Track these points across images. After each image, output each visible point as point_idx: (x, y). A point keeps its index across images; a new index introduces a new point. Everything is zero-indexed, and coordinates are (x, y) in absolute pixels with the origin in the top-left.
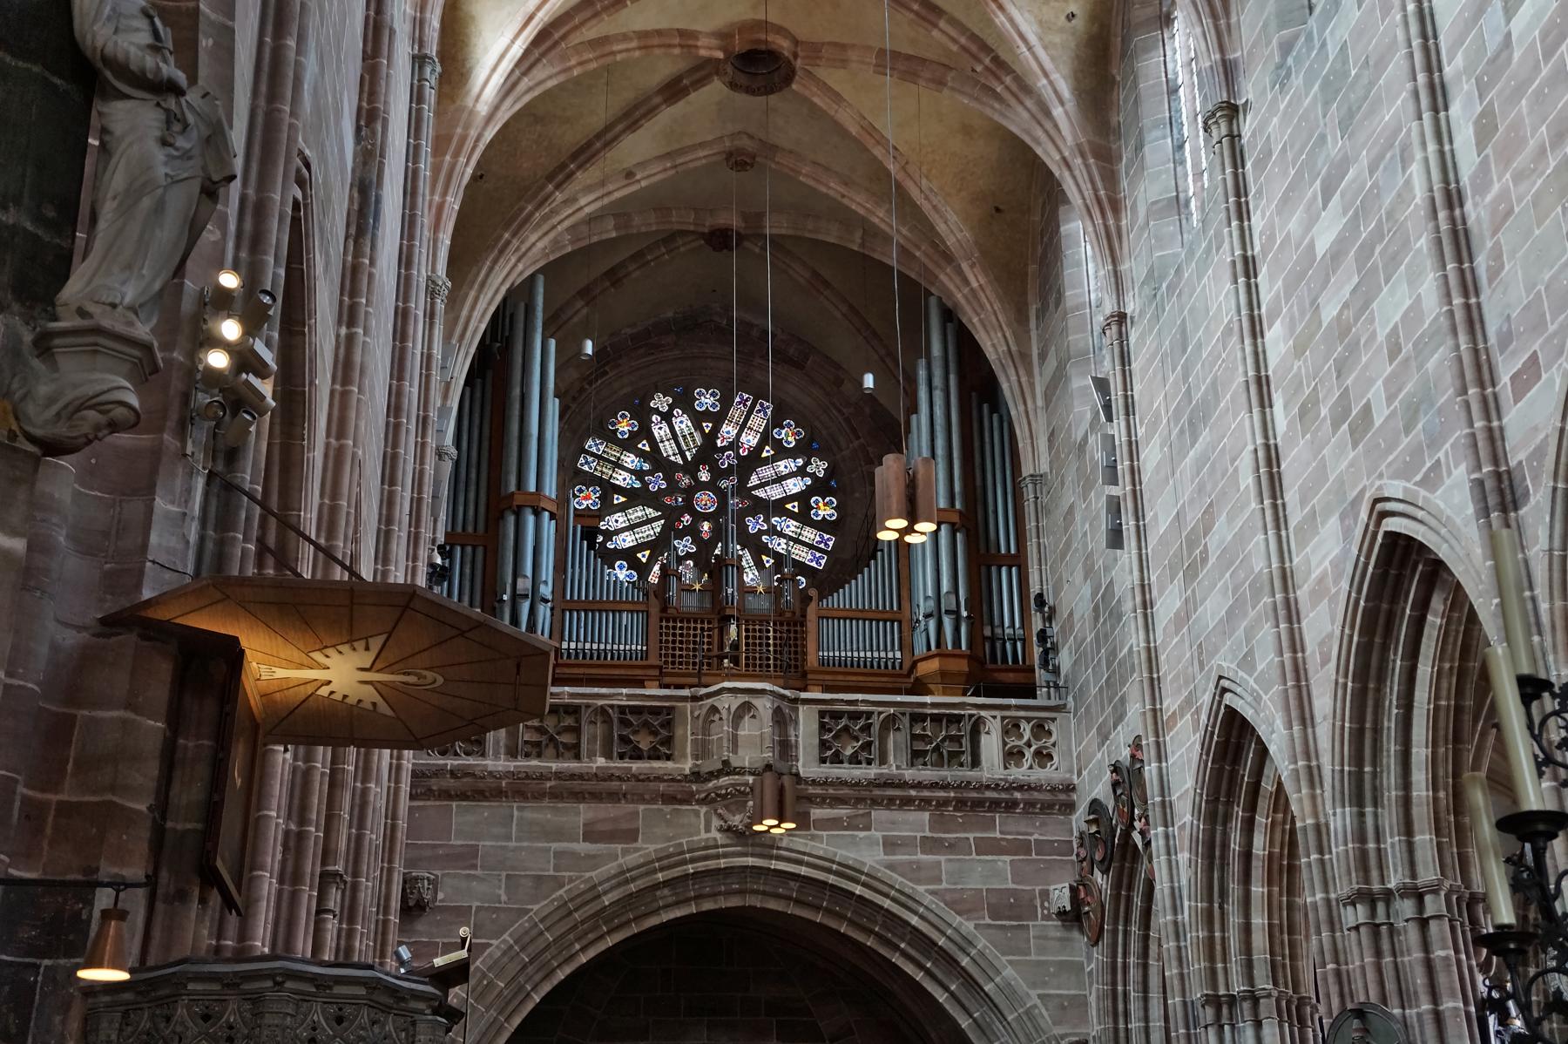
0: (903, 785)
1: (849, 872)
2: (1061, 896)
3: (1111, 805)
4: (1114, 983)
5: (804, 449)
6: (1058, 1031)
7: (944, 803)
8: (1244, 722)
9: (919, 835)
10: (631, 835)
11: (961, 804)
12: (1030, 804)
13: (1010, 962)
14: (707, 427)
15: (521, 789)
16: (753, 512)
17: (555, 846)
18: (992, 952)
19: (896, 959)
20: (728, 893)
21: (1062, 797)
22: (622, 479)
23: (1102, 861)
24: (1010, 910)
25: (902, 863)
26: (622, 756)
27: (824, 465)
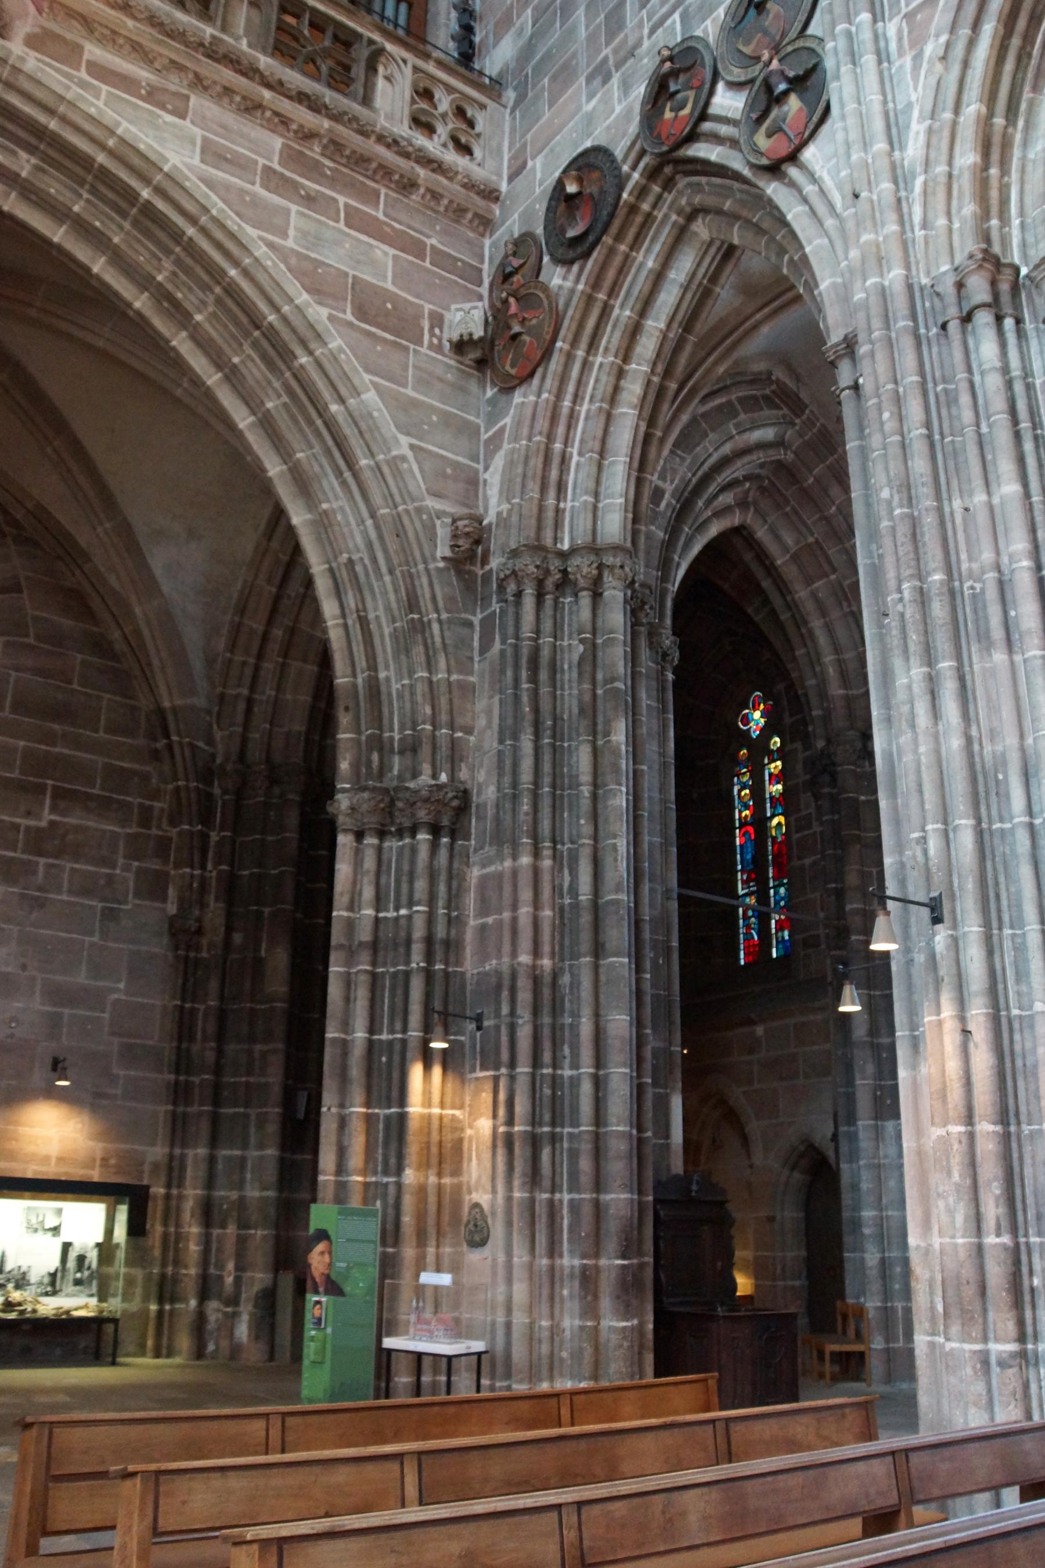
0: (250, 72)
4: (550, 437)
6: (431, 503)
7: (308, 136)
9: (262, 161)
11: (335, 147)
13: (376, 385)
18: (349, 360)
19: (181, 343)
25: (228, 187)
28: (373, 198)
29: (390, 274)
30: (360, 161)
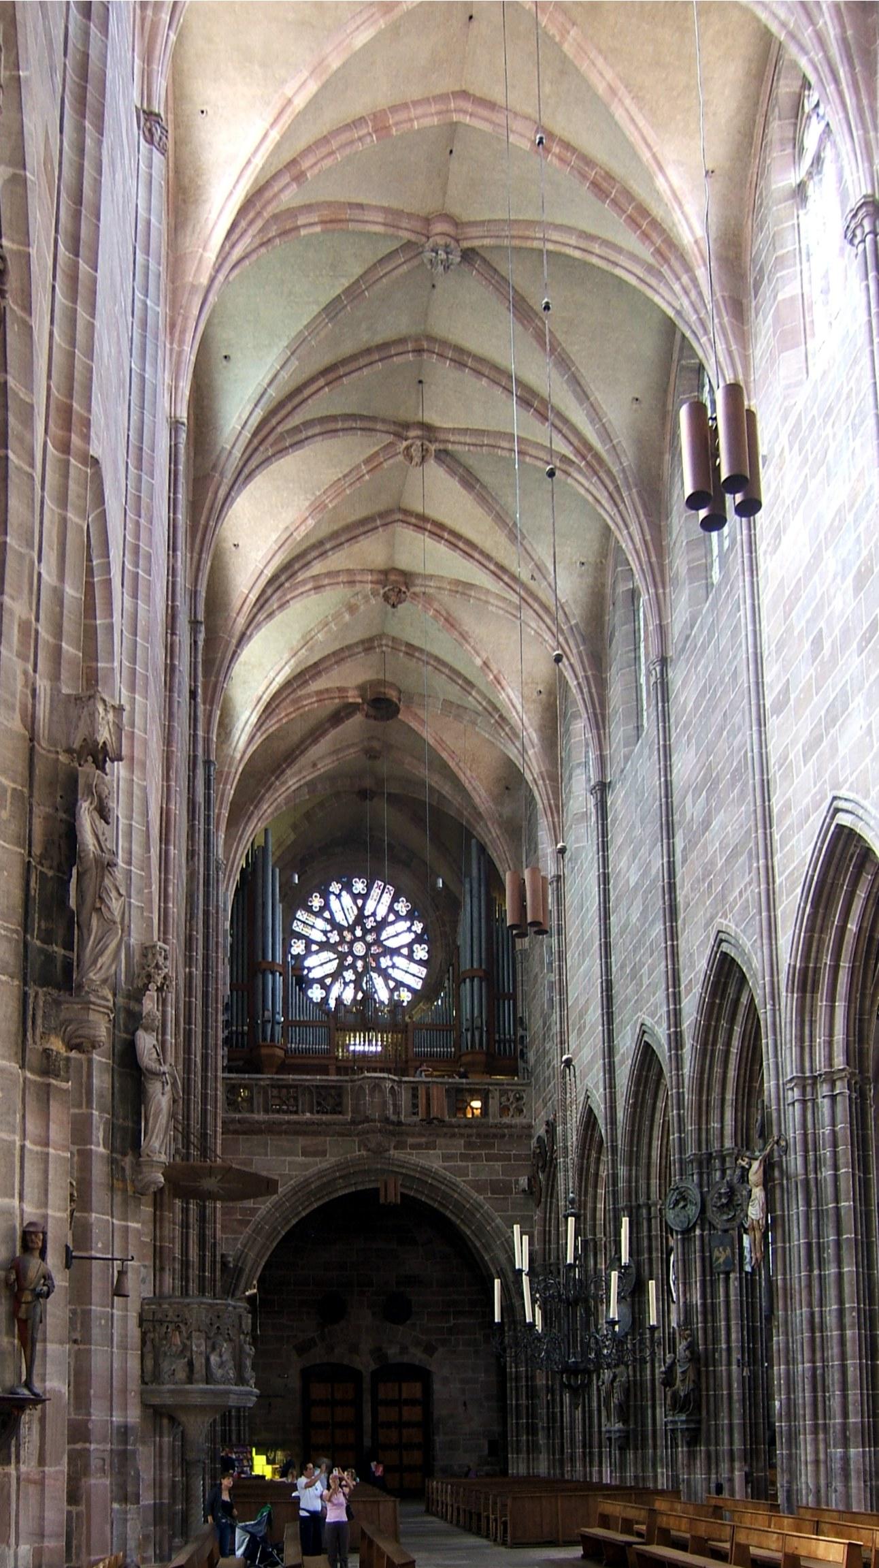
1: (426, 1171)
2: (524, 1181)
5: (410, 916)
7: (469, 1136)
8: (653, 1051)
10: (324, 1153)
11: (479, 1136)
12: (511, 1136)
14: (360, 902)
15: (271, 1129)
16: (384, 954)
17: (288, 1158)
19: (448, 1214)
20: (370, 1181)
21: (526, 1131)
22: (317, 936)
24: (500, 1189)
26: (318, 1112)
27: (421, 926)
28: (492, 1146)
30: (487, 1136)
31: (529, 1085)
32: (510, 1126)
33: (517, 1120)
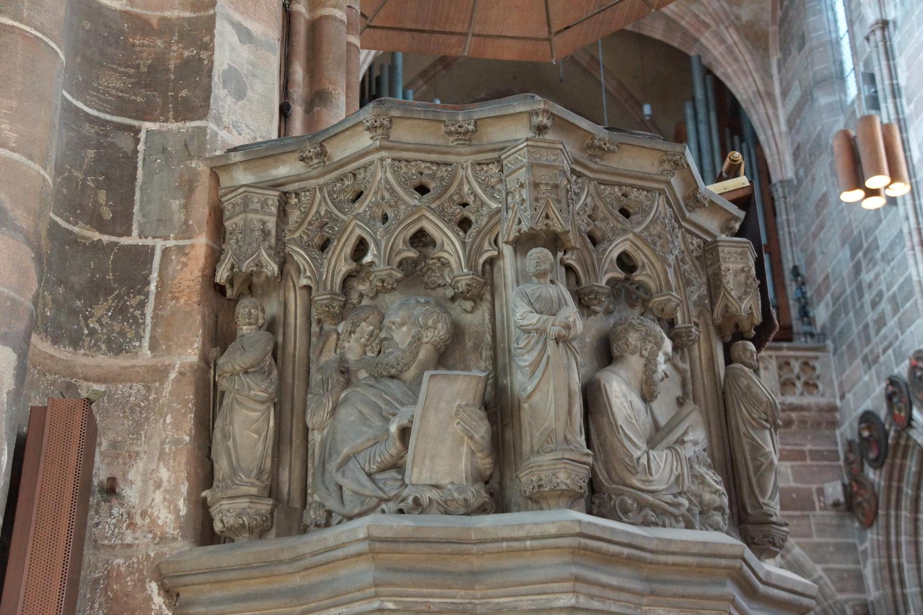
3: (883, 413)
12: (803, 422)
23: (876, 460)
29: (791, 477)
31: (823, 349)
32: (801, 408)
33: (809, 400)
